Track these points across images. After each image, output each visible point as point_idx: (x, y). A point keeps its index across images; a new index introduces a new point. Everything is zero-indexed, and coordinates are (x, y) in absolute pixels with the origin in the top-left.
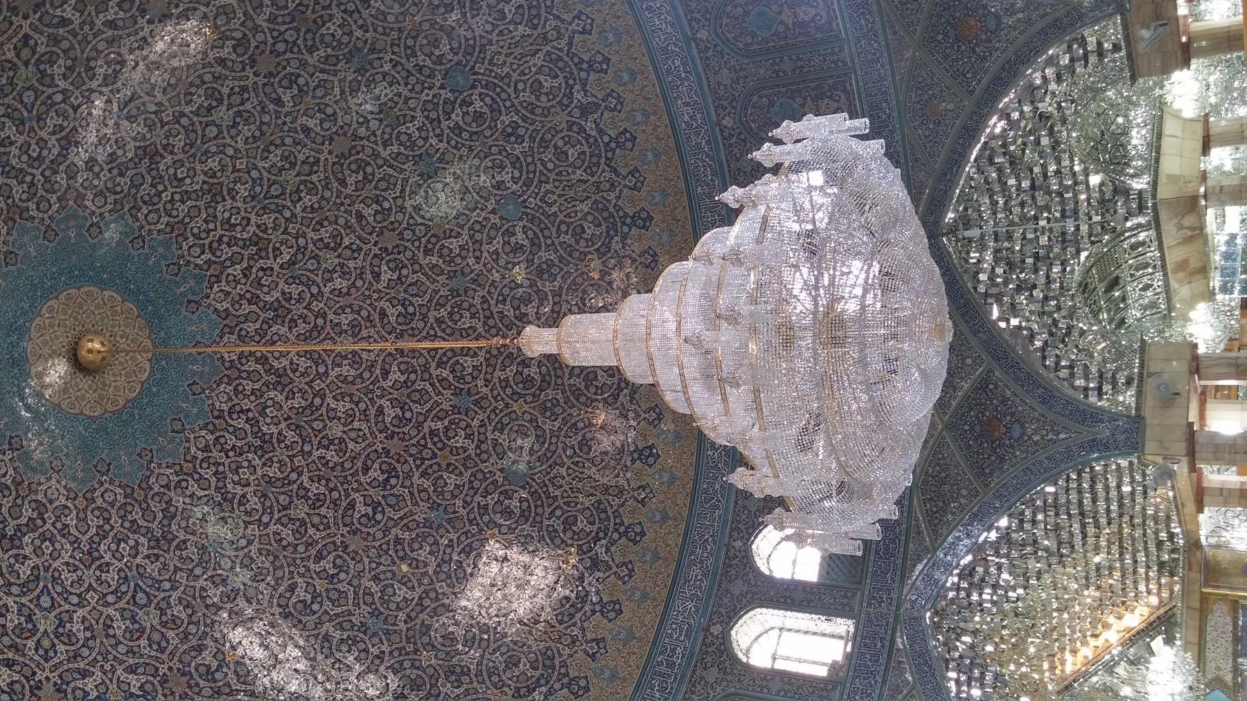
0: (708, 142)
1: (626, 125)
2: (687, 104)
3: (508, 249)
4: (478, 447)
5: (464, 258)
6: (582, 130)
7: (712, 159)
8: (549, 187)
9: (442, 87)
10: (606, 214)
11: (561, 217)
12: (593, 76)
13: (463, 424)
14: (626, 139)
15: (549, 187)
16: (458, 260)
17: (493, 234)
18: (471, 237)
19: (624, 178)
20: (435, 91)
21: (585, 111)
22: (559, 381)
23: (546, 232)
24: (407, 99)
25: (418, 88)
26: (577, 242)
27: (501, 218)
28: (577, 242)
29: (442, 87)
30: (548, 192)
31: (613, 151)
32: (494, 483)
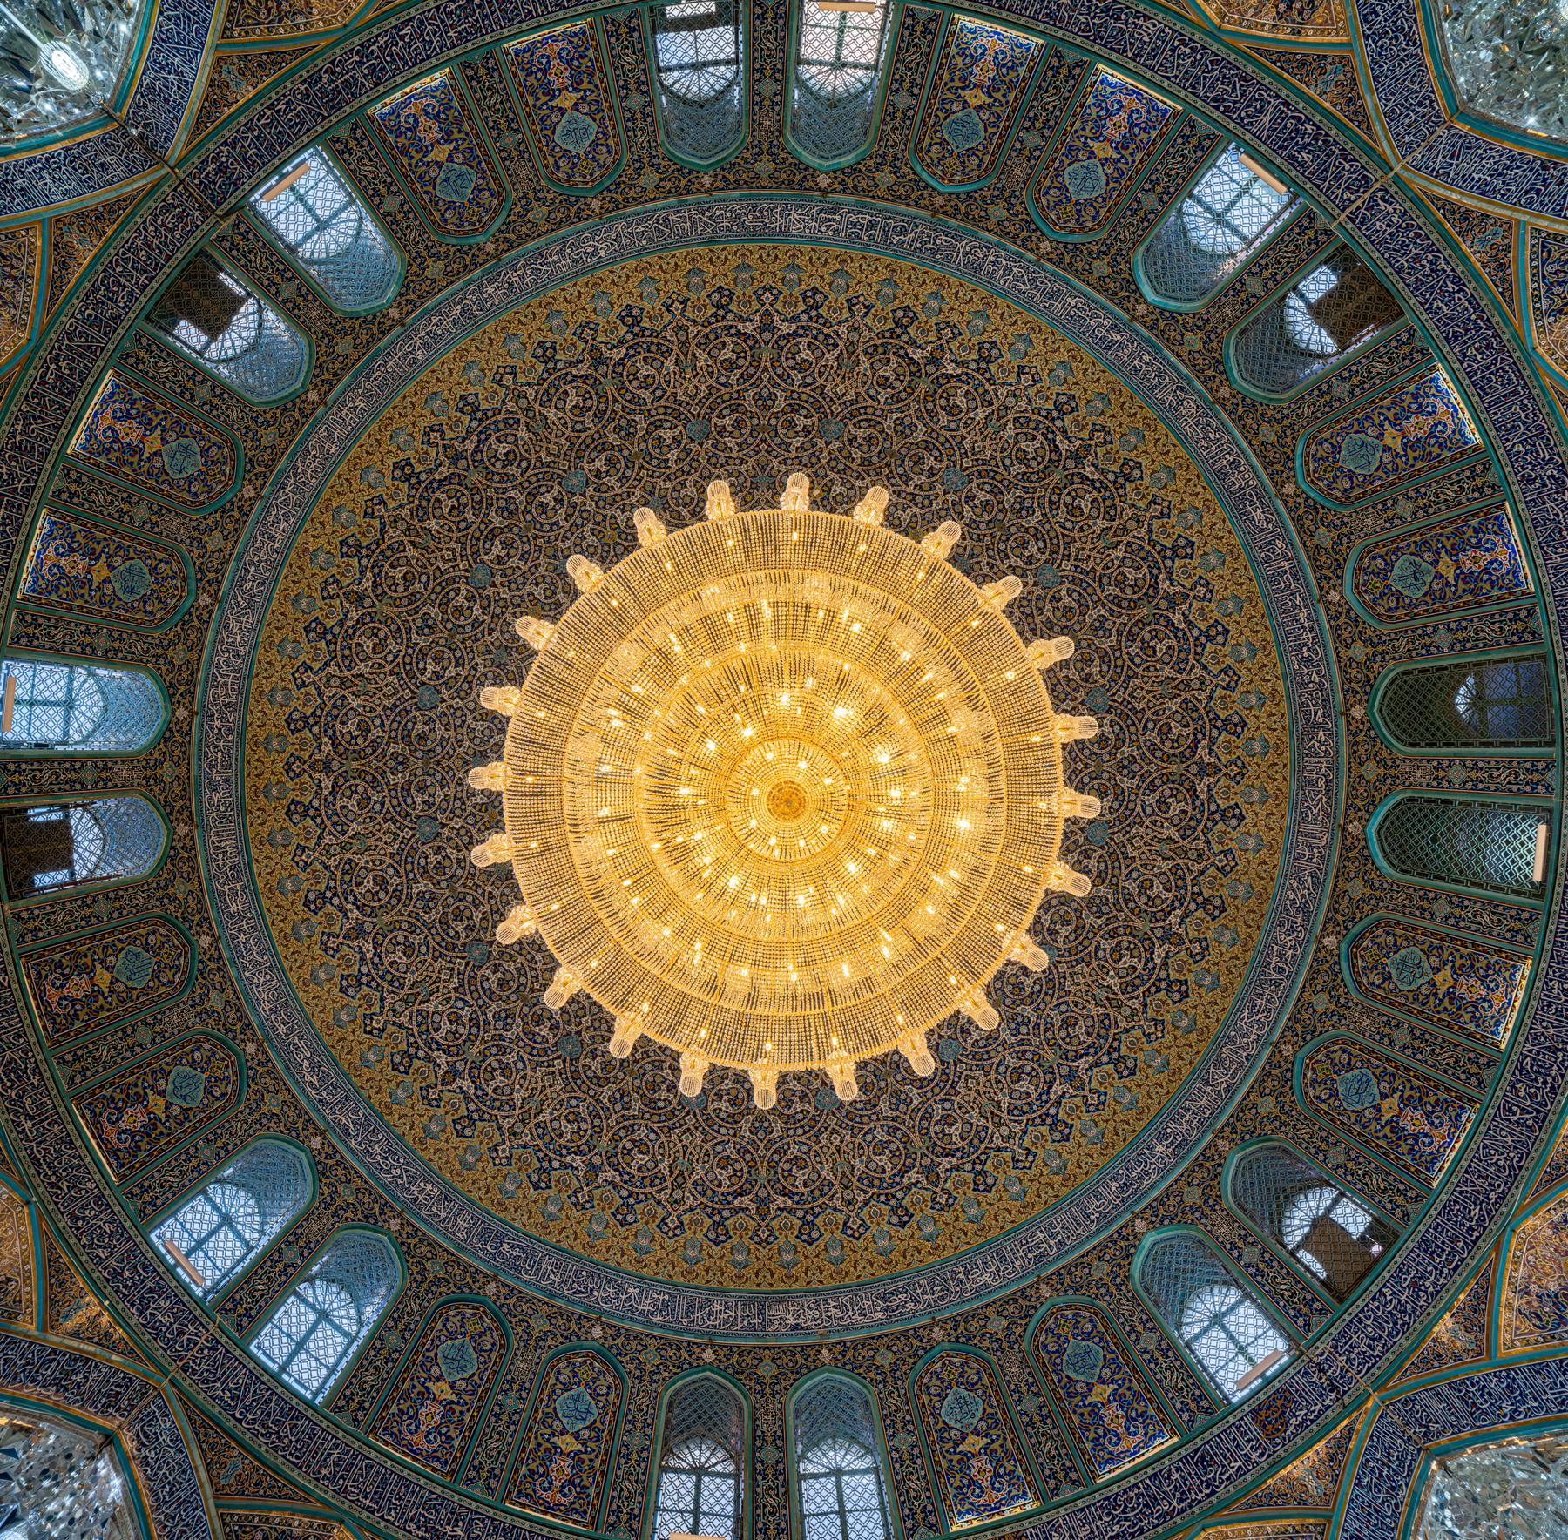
0: (284, 486)
1: (338, 560)
2: (271, 538)
3: (512, 552)
4: (689, 473)
5: (544, 577)
6: (375, 585)
7: (295, 468)
8: (440, 564)
9: (443, 700)
10: (424, 503)
11: (456, 534)
12: (330, 623)
13: (675, 495)
14: (349, 548)
15: (440, 564)
16: (548, 580)
17: (509, 572)
18: (524, 584)
19: (381, 517)
20: (450, 702)
21: (359, 599)
22: (597, 436)
23: (477, 534)
24: (472, 711)
25: (458, 713)
26: (466, 505)
27: (493, 575)
28: (466, 505)
29: (443, 700)
30: (445, 561)
31: (368, 547)
32: (715, 446)
